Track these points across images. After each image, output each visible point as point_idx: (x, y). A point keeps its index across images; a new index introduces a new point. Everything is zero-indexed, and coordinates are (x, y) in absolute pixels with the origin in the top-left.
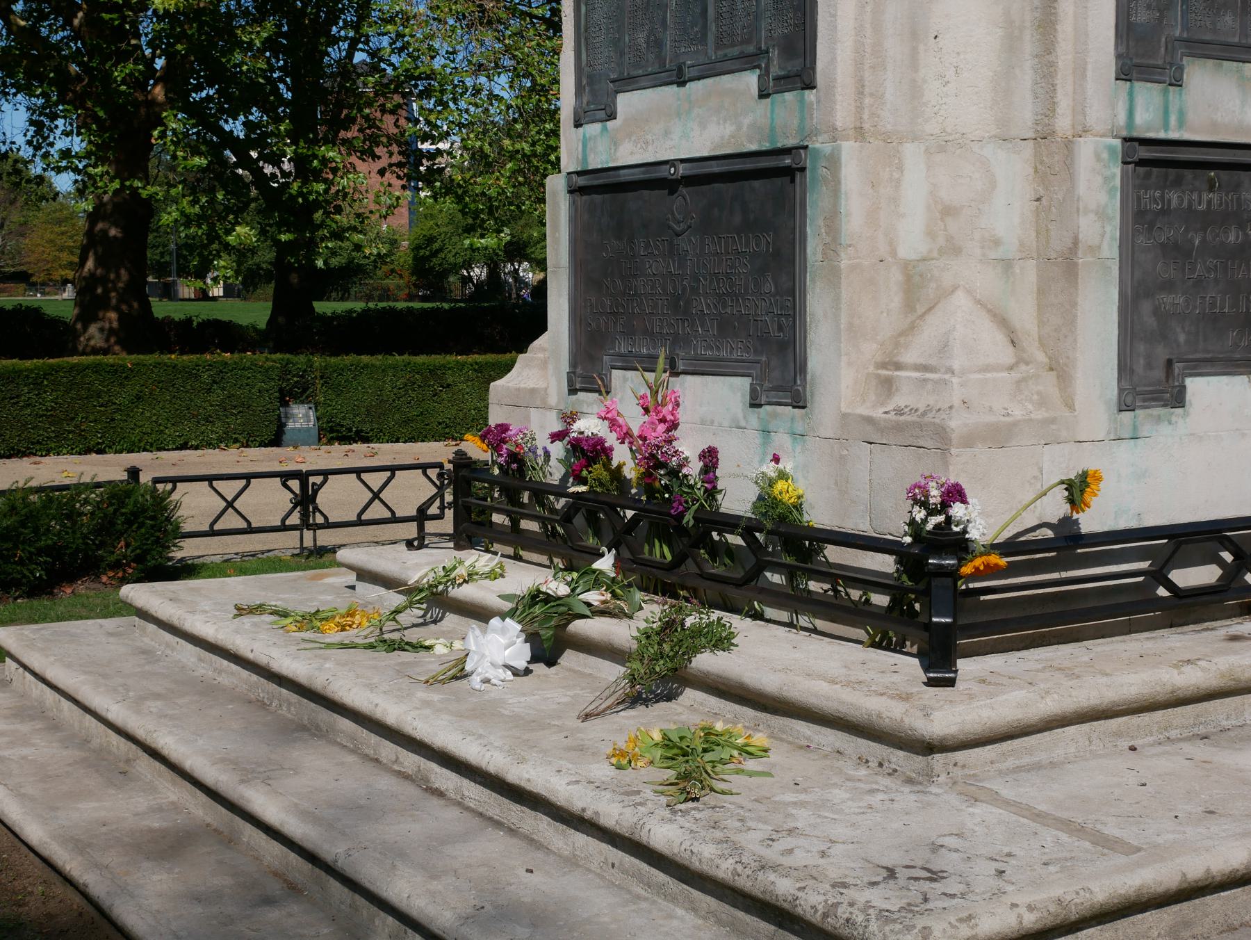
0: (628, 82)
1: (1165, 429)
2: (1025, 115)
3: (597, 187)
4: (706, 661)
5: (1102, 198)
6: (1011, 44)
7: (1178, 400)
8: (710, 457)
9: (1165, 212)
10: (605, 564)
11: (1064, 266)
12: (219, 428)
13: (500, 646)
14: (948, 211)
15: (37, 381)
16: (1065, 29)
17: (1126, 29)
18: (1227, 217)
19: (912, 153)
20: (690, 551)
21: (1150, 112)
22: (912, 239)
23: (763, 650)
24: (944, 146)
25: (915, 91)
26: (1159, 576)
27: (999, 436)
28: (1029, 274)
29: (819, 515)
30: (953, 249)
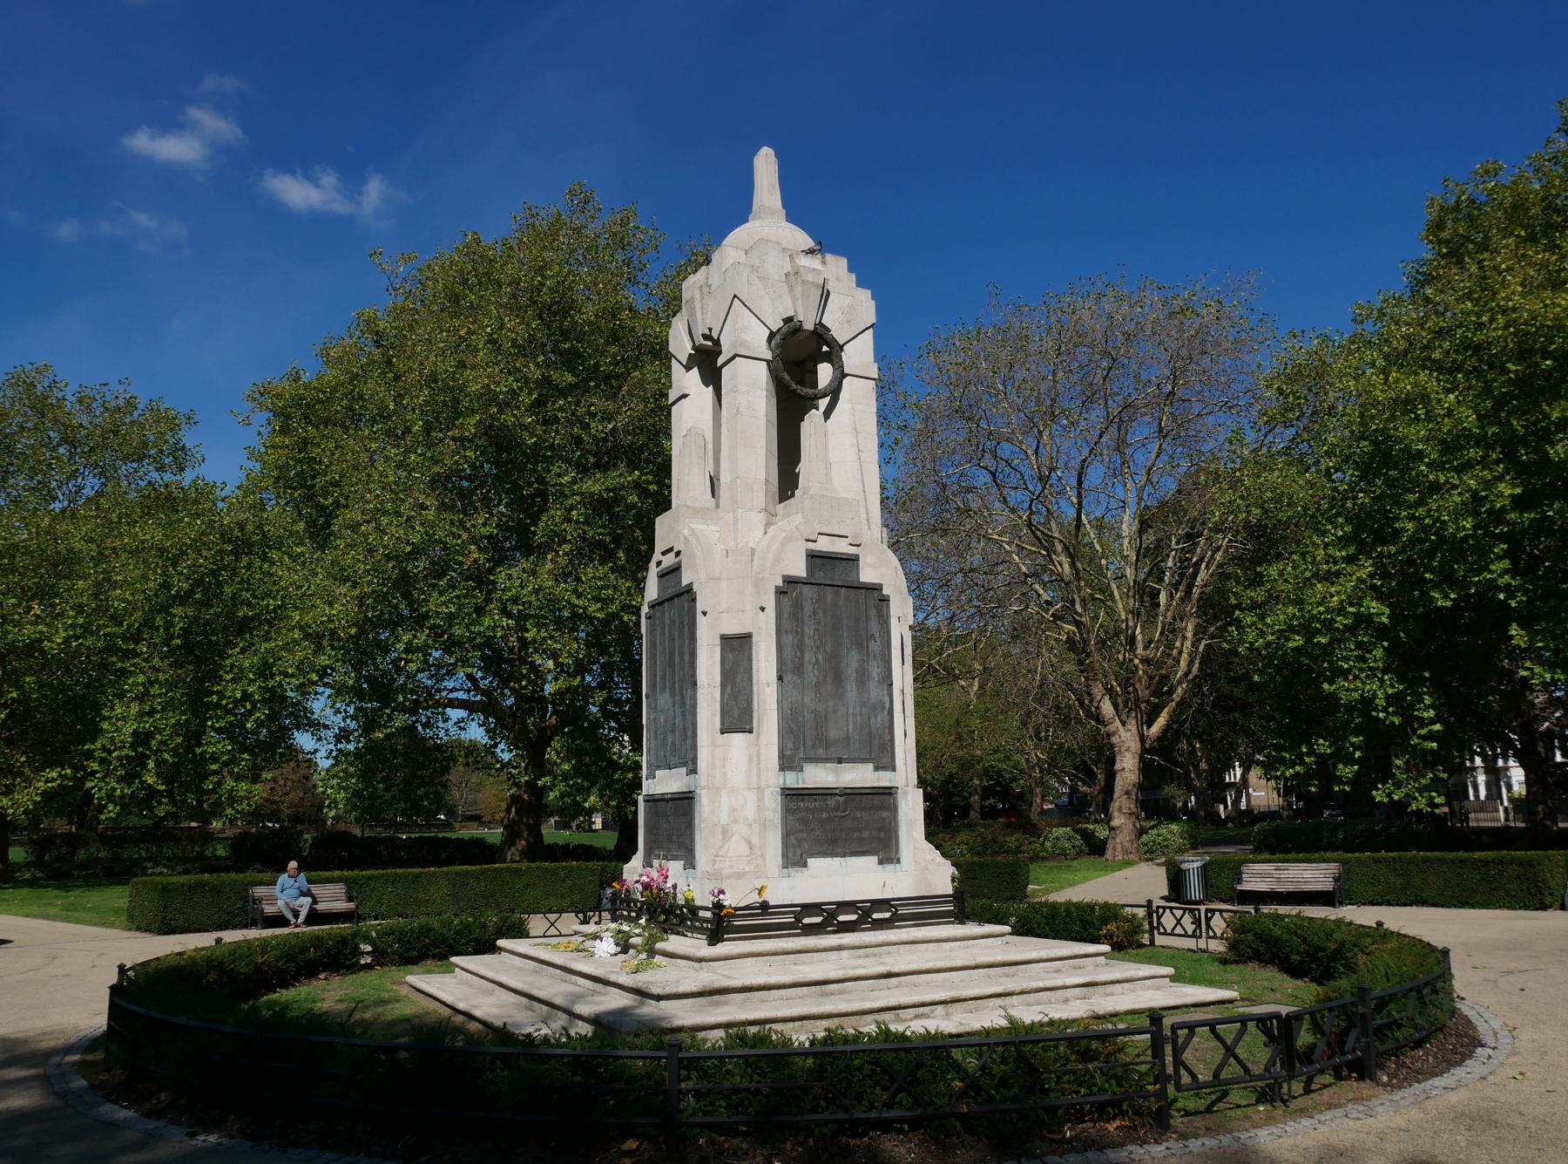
0: (658, 767)
2: (755, 781)
3: (651, 800)
4: (659, 945)
6: (751, 760)
7: (805, 865)
8: (675, 887)
9: (798, 809)
10: (642, 921)
11: (764, 826)
12: (568, 901)
13: (606, 946)
14: (734, 810)
15: (477, 876)
16: (763, 757)
17: (782, 756)
18: (822, 810)
19: (724, 792)
20: (667, 914)
21: (791, 780)
22: (724, 819)
23: (674, 943)
25: (724, 774)
26: (798, 920)
27: (740, 876)
28: (756, 829)
29: (698, 903)
30: (736, 821)
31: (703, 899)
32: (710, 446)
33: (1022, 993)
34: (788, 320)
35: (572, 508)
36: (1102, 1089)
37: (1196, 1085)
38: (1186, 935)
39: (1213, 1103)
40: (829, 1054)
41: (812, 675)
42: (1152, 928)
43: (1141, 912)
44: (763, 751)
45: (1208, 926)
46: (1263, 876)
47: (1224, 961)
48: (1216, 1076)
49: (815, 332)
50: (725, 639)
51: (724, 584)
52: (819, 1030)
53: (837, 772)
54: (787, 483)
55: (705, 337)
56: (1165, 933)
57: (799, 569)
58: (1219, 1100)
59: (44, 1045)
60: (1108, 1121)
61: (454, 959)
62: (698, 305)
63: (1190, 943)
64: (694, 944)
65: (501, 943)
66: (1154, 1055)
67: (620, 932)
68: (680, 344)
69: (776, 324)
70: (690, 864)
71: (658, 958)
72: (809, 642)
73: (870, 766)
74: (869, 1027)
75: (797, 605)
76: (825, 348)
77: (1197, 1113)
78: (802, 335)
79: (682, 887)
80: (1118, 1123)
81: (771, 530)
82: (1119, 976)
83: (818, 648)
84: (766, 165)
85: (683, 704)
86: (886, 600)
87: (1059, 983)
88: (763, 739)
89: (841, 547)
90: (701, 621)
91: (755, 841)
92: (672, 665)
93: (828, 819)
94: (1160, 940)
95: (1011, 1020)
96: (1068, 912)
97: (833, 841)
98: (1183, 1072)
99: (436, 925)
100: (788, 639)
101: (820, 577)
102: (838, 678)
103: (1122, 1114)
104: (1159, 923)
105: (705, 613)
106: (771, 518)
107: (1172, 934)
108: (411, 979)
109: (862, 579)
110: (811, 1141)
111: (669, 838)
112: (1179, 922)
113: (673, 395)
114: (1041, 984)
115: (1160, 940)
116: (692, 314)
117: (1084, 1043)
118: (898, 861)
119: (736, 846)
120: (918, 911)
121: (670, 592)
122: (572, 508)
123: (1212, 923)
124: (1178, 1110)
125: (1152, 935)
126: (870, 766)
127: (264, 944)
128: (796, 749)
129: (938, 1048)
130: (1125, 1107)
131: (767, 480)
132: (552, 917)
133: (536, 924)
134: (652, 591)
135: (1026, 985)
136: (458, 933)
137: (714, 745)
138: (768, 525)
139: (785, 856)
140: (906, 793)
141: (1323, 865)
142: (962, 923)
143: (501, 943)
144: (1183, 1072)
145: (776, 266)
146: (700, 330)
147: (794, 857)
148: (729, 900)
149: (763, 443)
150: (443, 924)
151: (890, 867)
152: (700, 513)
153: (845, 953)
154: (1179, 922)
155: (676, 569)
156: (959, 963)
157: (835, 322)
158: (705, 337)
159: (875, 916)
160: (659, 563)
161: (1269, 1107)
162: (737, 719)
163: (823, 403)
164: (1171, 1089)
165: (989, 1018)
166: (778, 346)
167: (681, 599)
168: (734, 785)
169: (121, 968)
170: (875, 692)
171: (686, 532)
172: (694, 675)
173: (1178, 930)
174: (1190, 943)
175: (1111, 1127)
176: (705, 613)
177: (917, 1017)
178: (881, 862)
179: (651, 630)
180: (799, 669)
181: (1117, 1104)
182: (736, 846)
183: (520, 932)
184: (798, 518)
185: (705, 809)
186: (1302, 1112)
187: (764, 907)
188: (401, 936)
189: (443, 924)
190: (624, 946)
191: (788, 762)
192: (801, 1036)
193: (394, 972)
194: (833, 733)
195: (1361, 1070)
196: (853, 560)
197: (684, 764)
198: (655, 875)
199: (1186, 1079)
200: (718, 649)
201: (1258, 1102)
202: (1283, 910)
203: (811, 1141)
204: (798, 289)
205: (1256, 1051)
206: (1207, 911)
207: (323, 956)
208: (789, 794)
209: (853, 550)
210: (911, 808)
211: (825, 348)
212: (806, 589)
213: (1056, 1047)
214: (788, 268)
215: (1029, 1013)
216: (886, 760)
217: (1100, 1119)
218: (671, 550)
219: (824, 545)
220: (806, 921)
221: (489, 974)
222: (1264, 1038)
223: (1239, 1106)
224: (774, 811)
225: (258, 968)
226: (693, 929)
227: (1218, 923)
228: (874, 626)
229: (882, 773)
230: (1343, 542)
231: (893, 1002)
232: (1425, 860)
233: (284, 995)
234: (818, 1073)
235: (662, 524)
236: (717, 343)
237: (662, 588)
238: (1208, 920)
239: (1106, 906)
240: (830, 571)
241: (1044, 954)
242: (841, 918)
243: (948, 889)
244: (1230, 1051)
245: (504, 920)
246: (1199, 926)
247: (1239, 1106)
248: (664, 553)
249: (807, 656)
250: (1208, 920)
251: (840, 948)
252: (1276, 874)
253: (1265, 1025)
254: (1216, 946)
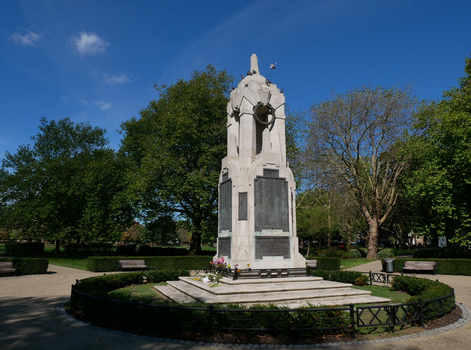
0: (222, 230)
3: (220, 239)
4: (220, 280)
5: (253, 241)
6: (247, 228)
7: (262, 258)
8: (226, 263)
10: (217, 273)
11: (250, 247)
13: (206, 280)
15: (181, 259)
18: (267, 243)
20: (224, 271)
21: (258, 234)
22: (239, 245)
23: (224, 279)
25: (239, 232)
26: (260, 274)
27: (243, 261)
29: (231, 268)
30: (242, 245)
31: (233, 267)
32: (237, 139)
33: (324, 297)
34: (259, 103)
35: (208, 156)
36: (334, 325)
37: (364, 325)
38: (381, 282)
39: (371, 332)
40: (255, 311)
41: (265, 204)
42: (371, 280)
43: (368, 275)
44: (250, 226)
45: (388, 280)
46: (412, 265)
47: (391, 290)
48: (370, 323)
49: (267, 106)
50: (240, 193)
51: (240, 178)
52: (251, 305)
53: (271, 232)
54: (259, 149)
55: (236, 108)
56: (375, 281)
57: (261, 174)
58: (373, 330)
59: (47, 299)
60: (337, 335)
61: (167, 282)
62: (234, 99)
63: (382, 284)
64: (229, 280)
65: (180, 278)
66: (351, 316)
67: (210, 275)
68: (230, 110)
69: (255, 104)
70: (230, 257)
71: (220, 284)
72: (264, 195)
73: (282, 230)
74: (266, 304)
75: (261, 184)
76: (270, 111)
77: (365, 334)
78: (263, 107)
79: (227, 264)
80: (339, 335)
81: (253, 163)
82: (354, 293)
84: (254, 59)
85: (229, 212)
87: (335, 294)
88: (250, 222)
89: (274, 167)
91: (248, 251)
92: (226, 201)
93: (269, 246)
94: (373, 283)
95: (309, 304)
96: (346, 274)
97: (270, 252)
98: (360, 321)
99: (164, 272)
100: (258, 194)
101: (267, 176)
102: (272, 205)
103: (341, 333)
104: (373, 278)
105: (234, 186)
106: (253, 159)
107: (377, 281)
108: (156, 287)
110: (249, 336)
111: (225, 250)
112: (379, 278)
113: (228, 124)
114: (330, 295)
115: (373, 283)
116: (232, 102)
117: (330, 312)
118: (290, 258)
119: (242, 252)
120: (296, 272)
121: (226, 180)
122: (208, 156)
123: (389, 278)
124: (360, 333)
125: (371, 281)
126: (282, 230)
127: (117, 276)
128: (260, 225)
129: (286, 311)
130: (341, 331)
131: (252, 149)
132: (197, 271)
133: (193, 273)
134: (221, 180)
135: (325, 295)
136: (170, 274)
137: (236, 224)
138: (252, 161)
139: (256, 256)
140: (292, 238)
141: (430, 262)
142: (309, 276)
143: (180, 278)
144: (360, 321)
145: (255, 87)
146: (235, 106)
147: (259, 256)
148: (239, 268)
149: (251, 138)
150: (166, 272)
151: (287, 259)
152: (234, 158)
153: (273, 284)
154: (379, 278)
155: (227, 174)
156: (306, 288)
157: (273, 103)
158: (236, 108)
159: (283, 273)
160: (223, 172)
161: (388, 333)
162: (243, 216)
163: (270, 126)
164: (356, 326)
165: (304, 304)
166: (256, 110)
167: (228, 182)
168: (241, 235)
169: (77, 280)
170: (283, 209)
171: (230, 163)
172: (231, 204)
173: (379, 280)
174: (382, 284)
175: (337, 336)
176: (234, 186)
177: (292, 303)
178: (284, 258)
179: (221, 191)
180: (261, 202)
181: (339, 330)
182: (242, 252)
183: (187, 275)
184: (261, 159)
185: (234, 241)
186: (398, 335)
187: (250, 270)
188: (155, 275)
189: (166, 272)
190: (212, 280)
191: (257, 229)
192: (248, 306)
193: (152, 284)
194: (271, 221)
195: (419, 323)
196: (277, 171)
197: (229, 229)
198: (220, 260)
199: (361, 324)
201: (385, 331)
202: (409, 275)
203: (249, 336)
204: (262, 94)
205: (383, 316)
206: (388, 275)
207: (133, 280)
208: (257, 238)
209: (277, 168)
210: (294, 243)
211: (270, 111)
213: (322, 313)
214: (259, 88)
215: (315, 303)
216: (286, 229)
217: (334, 334)
218: (225, 168)
219: (269, 167)
220: (262, 274)
221: (174, 286)
222: (387, 313)
223: (379, 332)
225: (114, 282)
226: (230, 275)
227: (391, 279)
228: (283, 190)
229: (285, 232)
230: (438, 164)
231: (284, 298)
232: (462, 261)
233: (121, 290)
234: (251, 317)
235: (224, 161)
236: (239, 110)
237: (223, 179)
238: (388, 277)
239: (357, 272)
240: (270, 174)
241: (332, 286)
242: (272, 274)
244: (375, 316)
245: (184, 271)
246: (385, 279)
247: (379, 332)
248: (224, 169)
249: (263, 199)
250: (388, 277)
251: (271, 282)
252: (415, 264)
253: (386, 309)
254: (390, 286)
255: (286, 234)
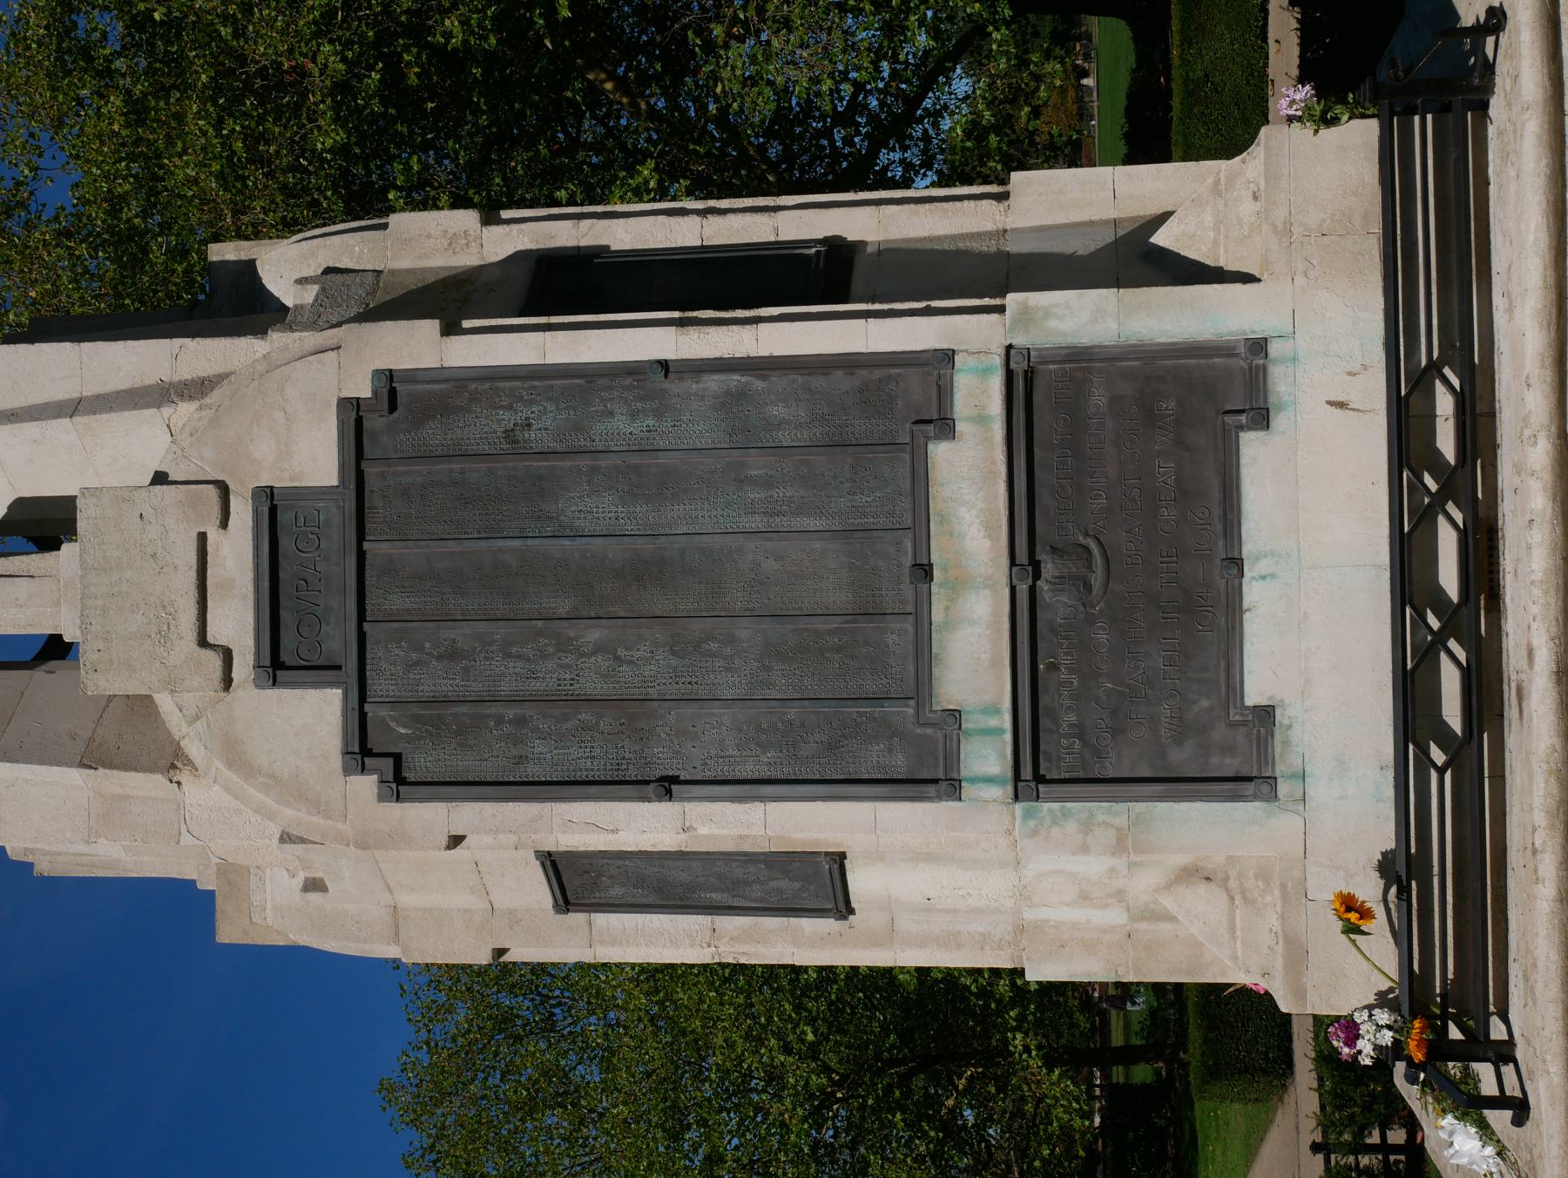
1: (1296, 734)
7: (1266, 714)
19: (1029, 915)
21: (986, 757)
24: (1024, 895)
41: (650, 665)
50: (565, 902)
51: (407, 900)
53: (959, 586)
57: (318, 712)
72: (548, 678)
73: (939, 451)
83: (564, 646)
86: (390, 384)
89: (235, 554)
90: (522, 952)
101: (337, 639)
102: (649, 571)
109: (335, 482)
118: (1259, 346)
126: (939, 451)
151: (1280, 381)
170: (695, 425)
180: (632, 709)
187: (1402, 870)
191: (931, 776)
196: (274, 508)
200: (600, 919)
208: (1033, 775)
209: (242, 511)
212: (380, 686)
219: (235, 621)
224: (1087, 827)
228: (481, 428)
229: (962, 405)
243: (1359, 136)
249: (593, 686)
255: (979, 397)
